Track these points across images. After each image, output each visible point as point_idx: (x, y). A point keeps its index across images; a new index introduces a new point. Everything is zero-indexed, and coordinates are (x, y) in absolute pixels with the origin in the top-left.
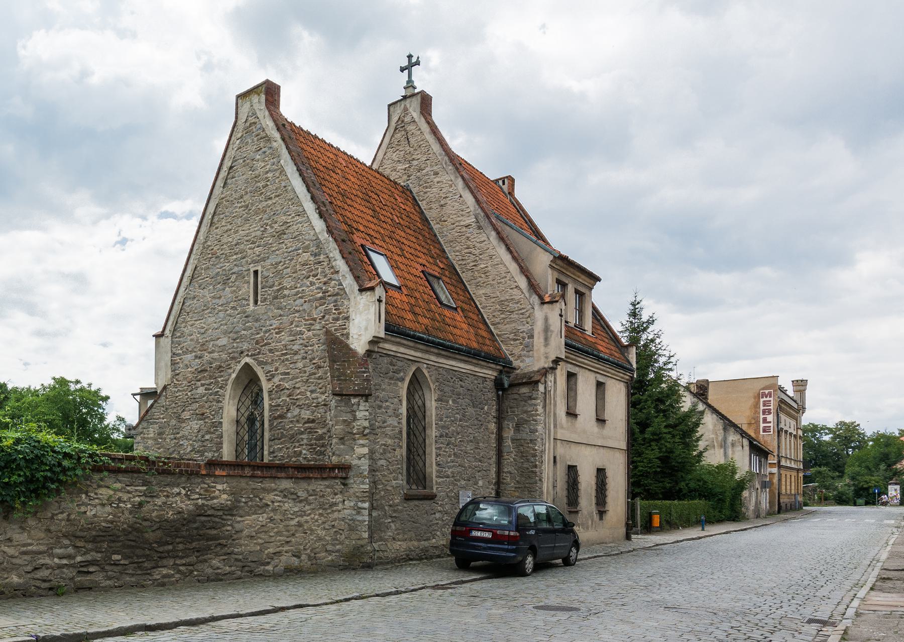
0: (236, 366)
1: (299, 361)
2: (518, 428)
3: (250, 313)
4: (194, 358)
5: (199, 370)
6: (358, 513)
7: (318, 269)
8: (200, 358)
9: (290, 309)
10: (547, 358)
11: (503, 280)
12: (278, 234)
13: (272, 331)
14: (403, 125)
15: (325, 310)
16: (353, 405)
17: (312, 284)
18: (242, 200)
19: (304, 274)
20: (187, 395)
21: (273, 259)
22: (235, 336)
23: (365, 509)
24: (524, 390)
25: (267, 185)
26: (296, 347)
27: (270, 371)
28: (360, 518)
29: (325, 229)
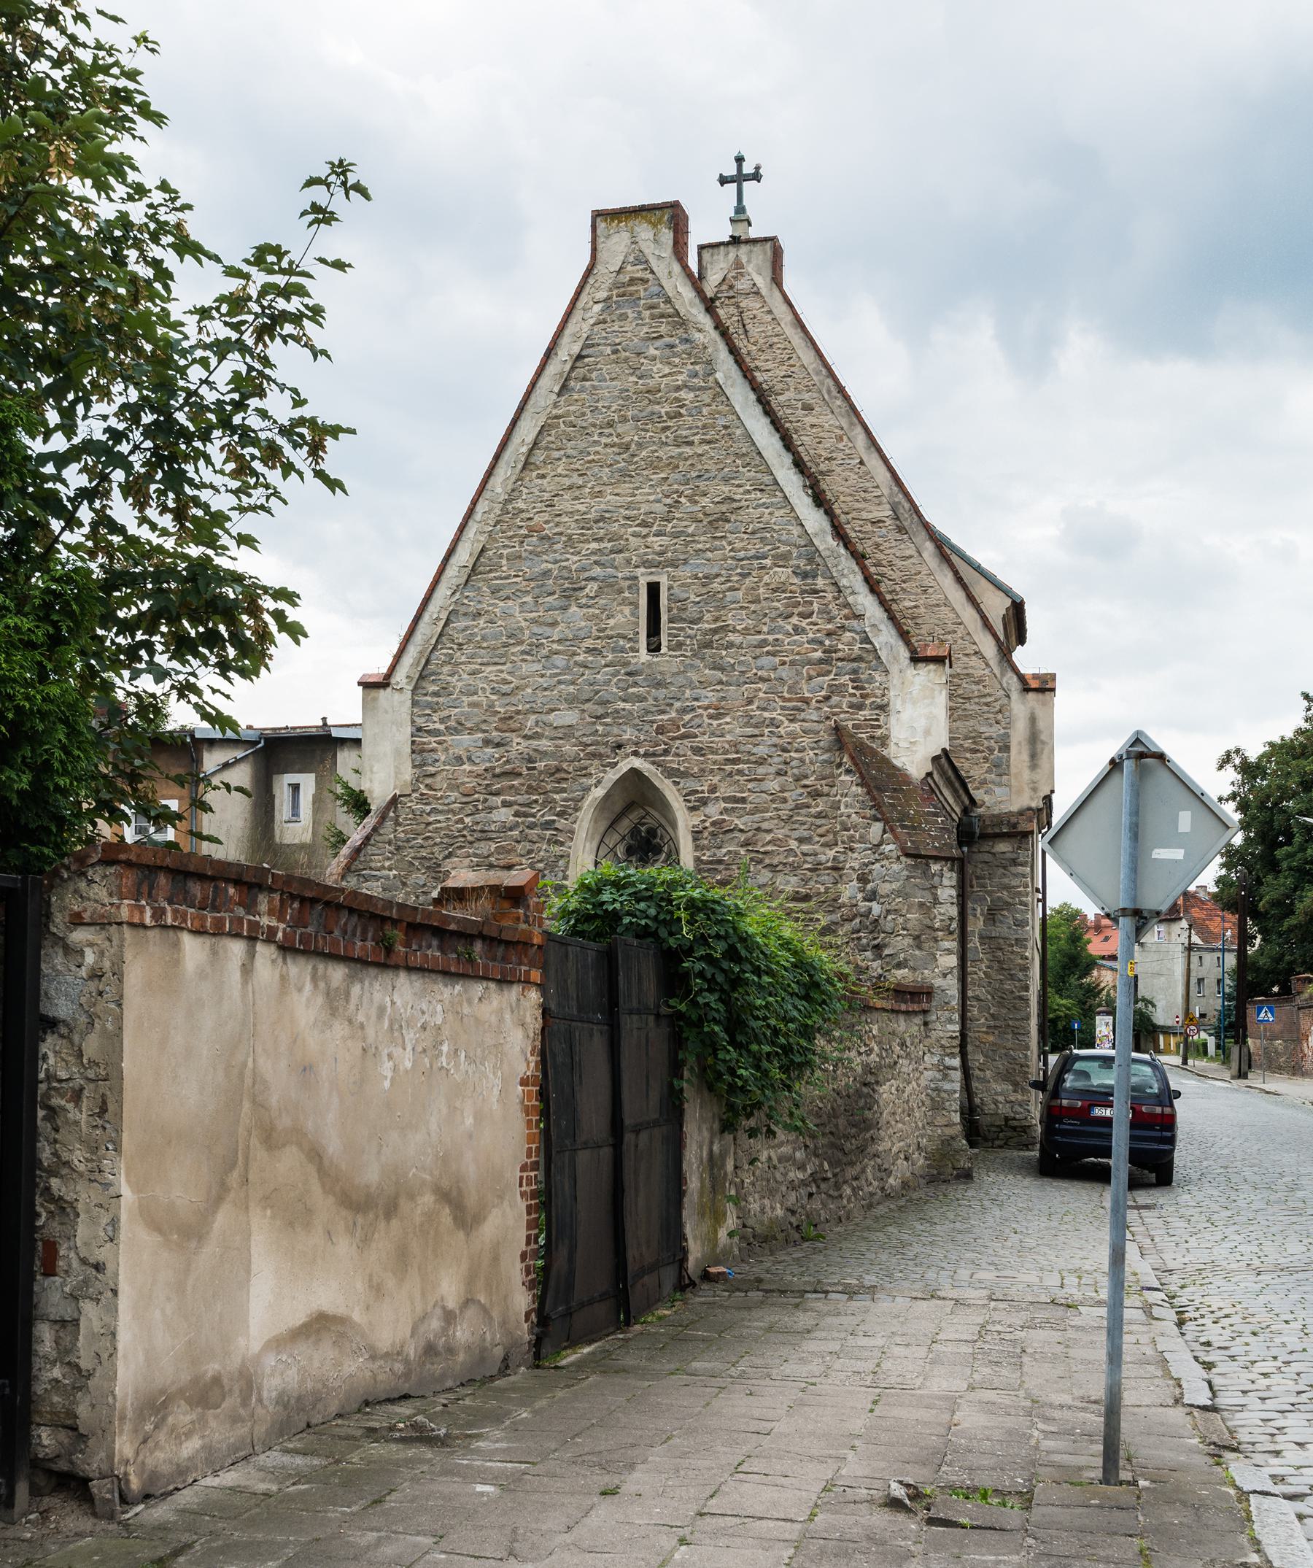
0: (605, 772)
1: (771, 777)
2: (992, 916)
3: (638, 667)
4: (480, 744)
5: (498, 771)
6: (945, 1077)
7: (811, 603)
8: (498, 745)
9: (743, 672)
10: (1035, 790)
11: (949, 637)
12: (710, 518)
13: (700, 711)
14: (731, 294)
15: (829, 686)
16: (934, 875)
17: (802, 631)
18: (610, 430)
19: (777, 609)
20: (461, 821)
21: (698, 566)
22: (600, 711)
23: (955, 1069)
24: (1003, 847)
25: (681, 415)
26: (761, 750)
27: (697, 792)
28: (947, 1086)
29: (828, 528)
